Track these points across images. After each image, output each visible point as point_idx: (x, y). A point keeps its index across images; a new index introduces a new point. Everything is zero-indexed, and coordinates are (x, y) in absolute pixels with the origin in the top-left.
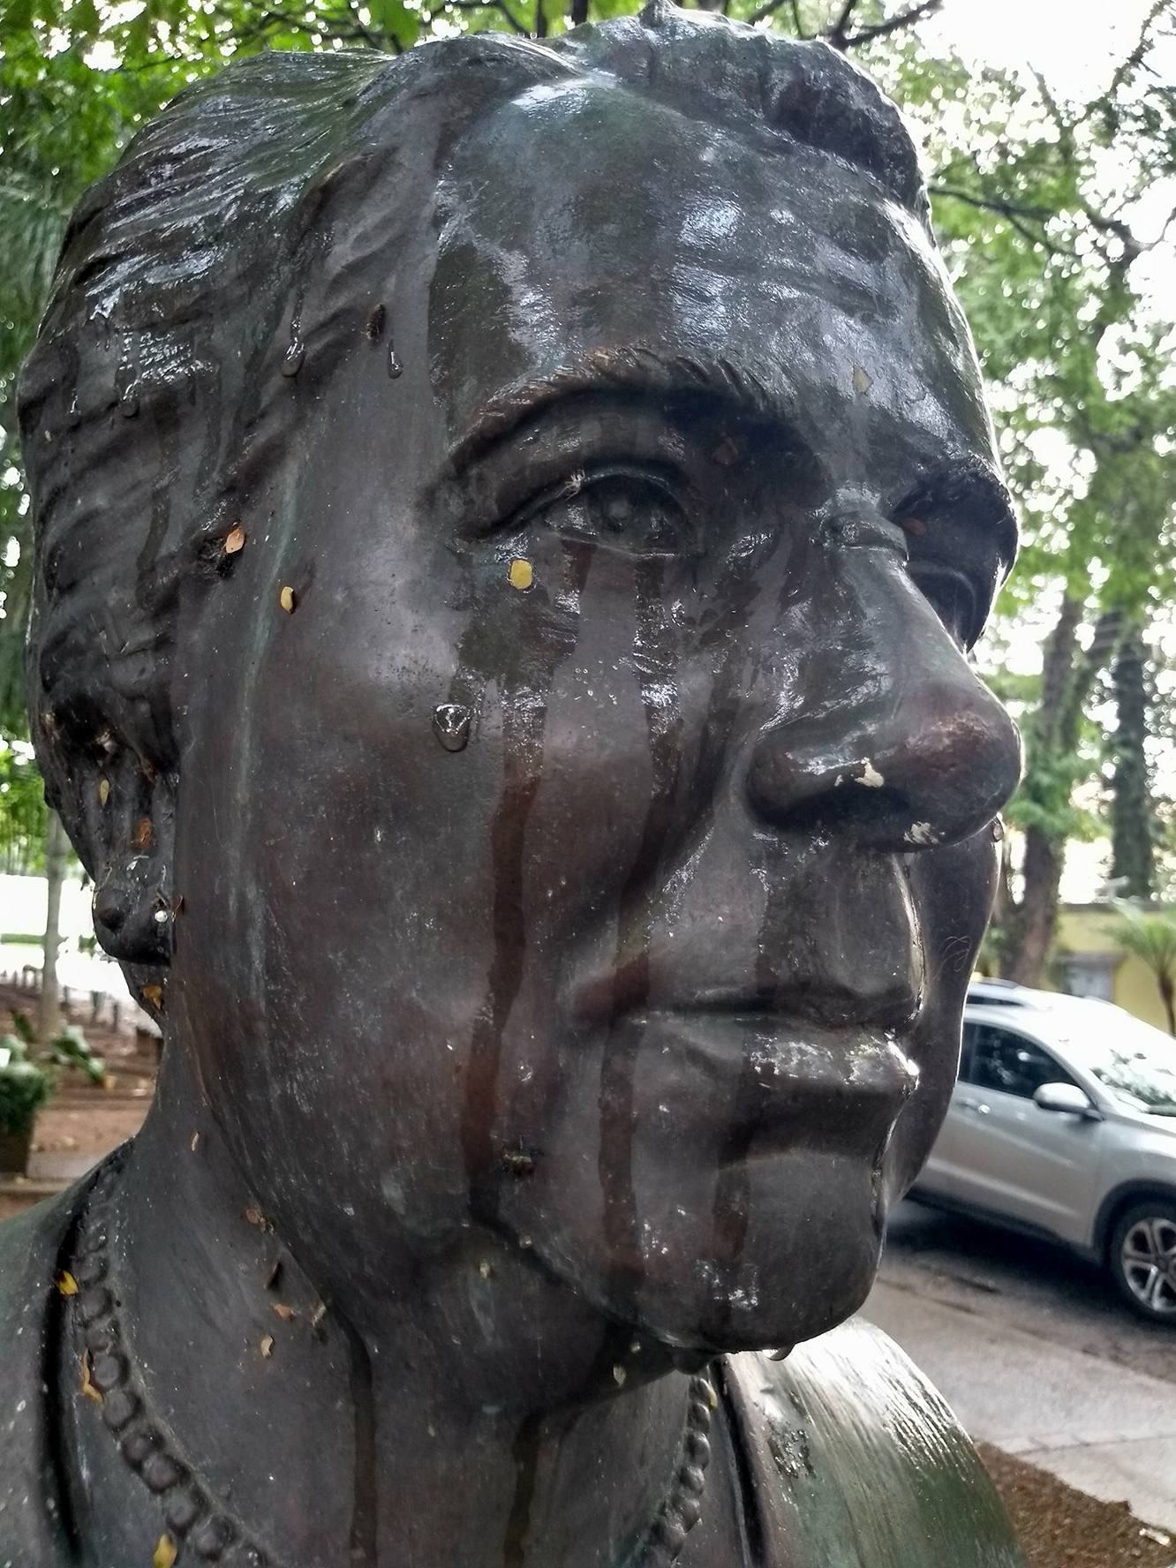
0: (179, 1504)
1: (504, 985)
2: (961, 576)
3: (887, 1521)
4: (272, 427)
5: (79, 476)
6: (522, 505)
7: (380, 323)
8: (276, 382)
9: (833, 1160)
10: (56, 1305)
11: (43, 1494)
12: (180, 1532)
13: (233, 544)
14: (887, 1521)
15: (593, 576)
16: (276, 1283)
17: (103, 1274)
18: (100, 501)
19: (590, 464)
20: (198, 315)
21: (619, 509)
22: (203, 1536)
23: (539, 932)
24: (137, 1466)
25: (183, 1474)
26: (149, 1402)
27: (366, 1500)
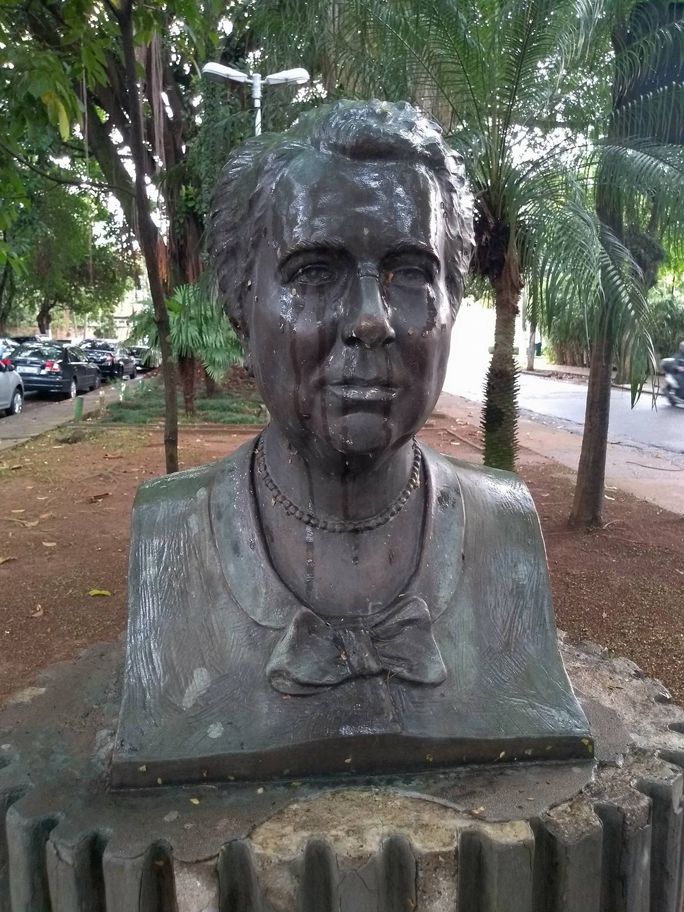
0: (275, 492)
1: (298, 382)
3: (483, 524)
4: (251, 256)
5: (221, 266)
6: (293, 275)
7: (265, 232)
8: (250, 246)
9: (370, 415)
10: (254, 455)
11: (250, 490)
12: (275, 498)
13: (249, 284)
14: (483, 524)
15: (308, 291)
16: (290, 447)
17: (262, 449)
18: (226, 272)
19: (302, 267)
20: (235, 228)
21: (313, 273)
22: (279, 498)
23: (302, 371)
24: (267, 486)
25: (276, 487)
26: (270, 474)
27: (311, 494)
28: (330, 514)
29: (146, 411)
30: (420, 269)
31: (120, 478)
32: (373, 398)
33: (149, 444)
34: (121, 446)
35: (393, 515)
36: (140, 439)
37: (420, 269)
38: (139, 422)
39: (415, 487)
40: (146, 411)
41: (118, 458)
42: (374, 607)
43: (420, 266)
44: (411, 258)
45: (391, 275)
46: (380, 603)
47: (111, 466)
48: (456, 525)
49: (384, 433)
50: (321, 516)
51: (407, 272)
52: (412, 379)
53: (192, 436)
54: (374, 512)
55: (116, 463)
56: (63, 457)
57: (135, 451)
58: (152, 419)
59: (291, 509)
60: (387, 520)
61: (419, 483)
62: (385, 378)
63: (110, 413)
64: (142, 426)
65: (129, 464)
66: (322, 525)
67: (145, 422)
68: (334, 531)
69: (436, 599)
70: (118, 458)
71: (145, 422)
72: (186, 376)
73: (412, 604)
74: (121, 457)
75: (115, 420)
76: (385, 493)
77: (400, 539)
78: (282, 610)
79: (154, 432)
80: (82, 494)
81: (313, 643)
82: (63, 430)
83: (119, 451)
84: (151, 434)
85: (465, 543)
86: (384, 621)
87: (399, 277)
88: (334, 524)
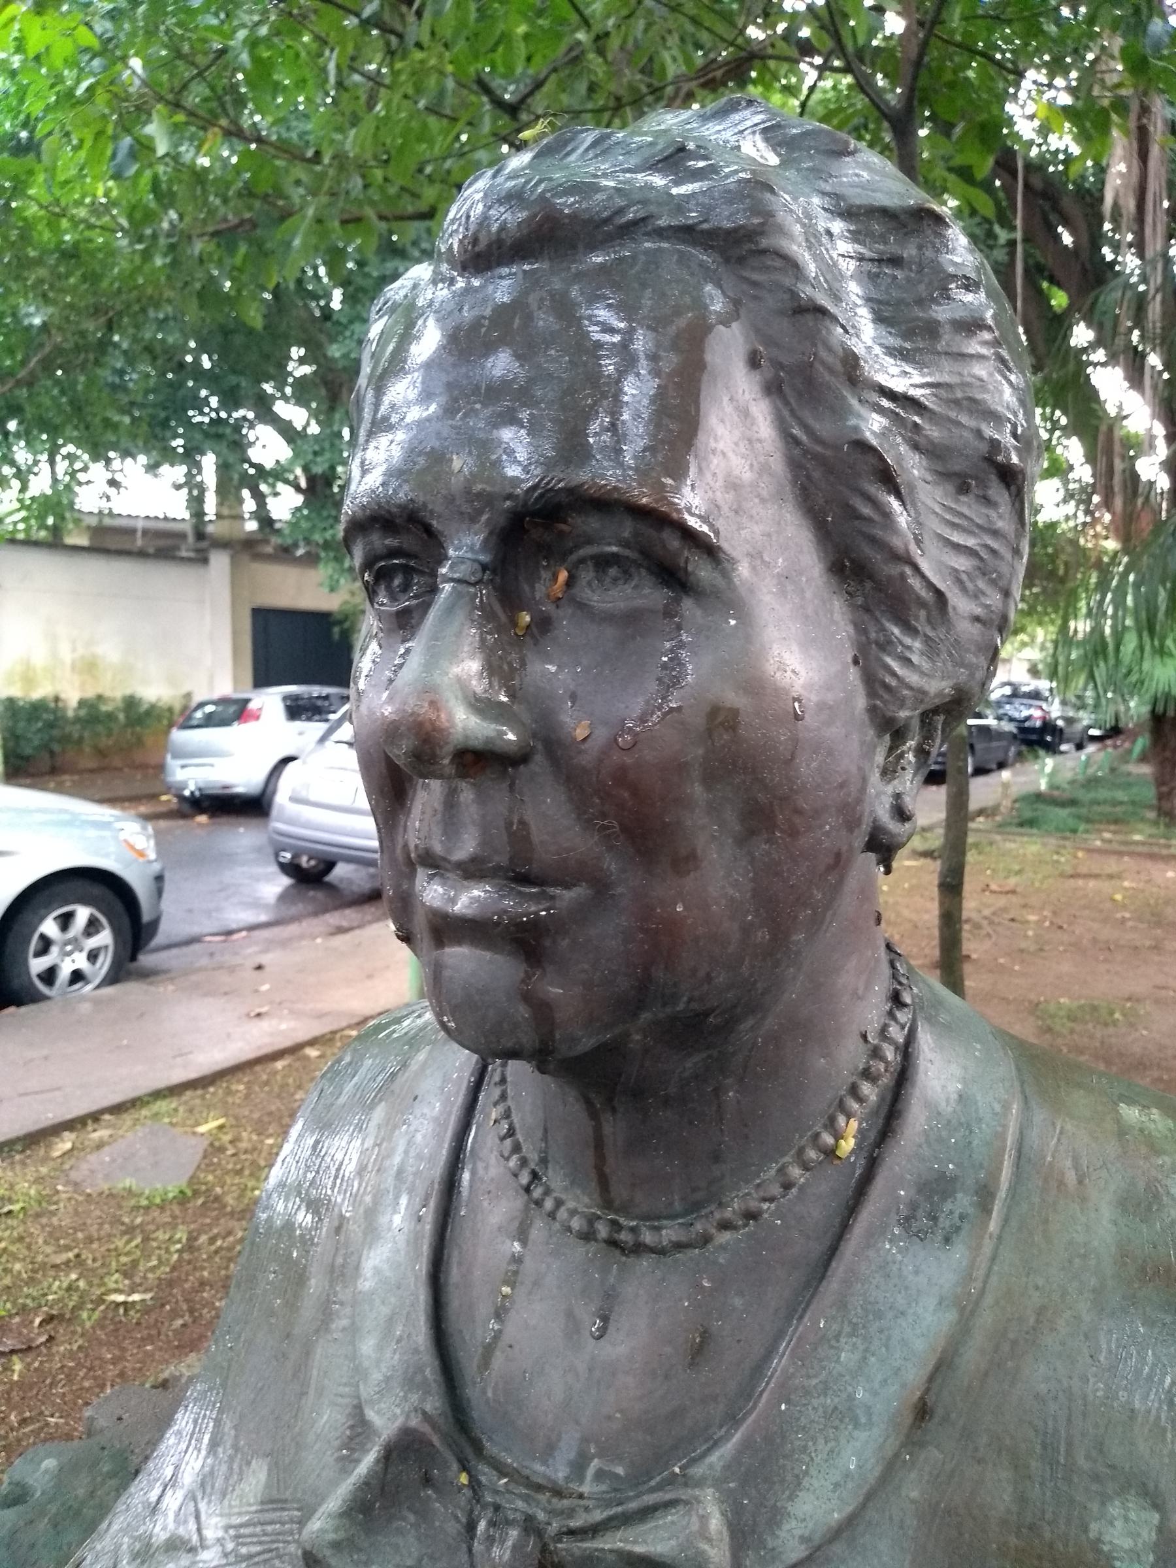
2: (614, 549)
9: (487, 955)
28: (573, 1183)
29: (1084, 811)
30: (627, 552)
31: (999, 929)
32: (469, 912)
33: (1069, 869)
34: (1019, 872)
35: (725, 1226)
36: (1057, 862)
37: (627, 552)
38: (1063, 831)
39: (830, 1153)
40: (1084, 811)
41: (1007, 893)
42: (600, 1475)
43: (625, 544)
44: (592, 523)
45: (563, 575)
46: (620, 1470)
47: (988, 906)
48: (931, 1302)
49: (523, 1012)
50: (555, 1178)
51: (603, 563)
52: (611, 864)
53: (1161, 865)
54: (678, 1206)
55: (1002, 901)
56: (914, 881)
57: (1042, 883)
58: (1089, 826)
59: (508, 1142)
60: (706, 1240)
61: (847, 1145)
62: (502, 859)
63: (1018, 810)
64: (1065, 838)
65: (1025, 906)
66: (549, 1204)
67: (1074, 831)
68: (569, 1229)
69: (776, 1517)
70: (1007, 893)
71: (1074, 831)
72: (1164, 749)
73: (681, 1509)
74: (1013, 892)
75: (1021, 825)
76: (716, 1158)
77: (738, 1302)
78: (405, 1398)
79: (1090, 851)
80: (927, 951)
81: (424, 1514)
82: (928, 835)
83: (1012, 881)
84: (1080, 854)
85: (943, 1367)
86: (594, 1530)
87: (587, 575)
88: (573, 1213)
